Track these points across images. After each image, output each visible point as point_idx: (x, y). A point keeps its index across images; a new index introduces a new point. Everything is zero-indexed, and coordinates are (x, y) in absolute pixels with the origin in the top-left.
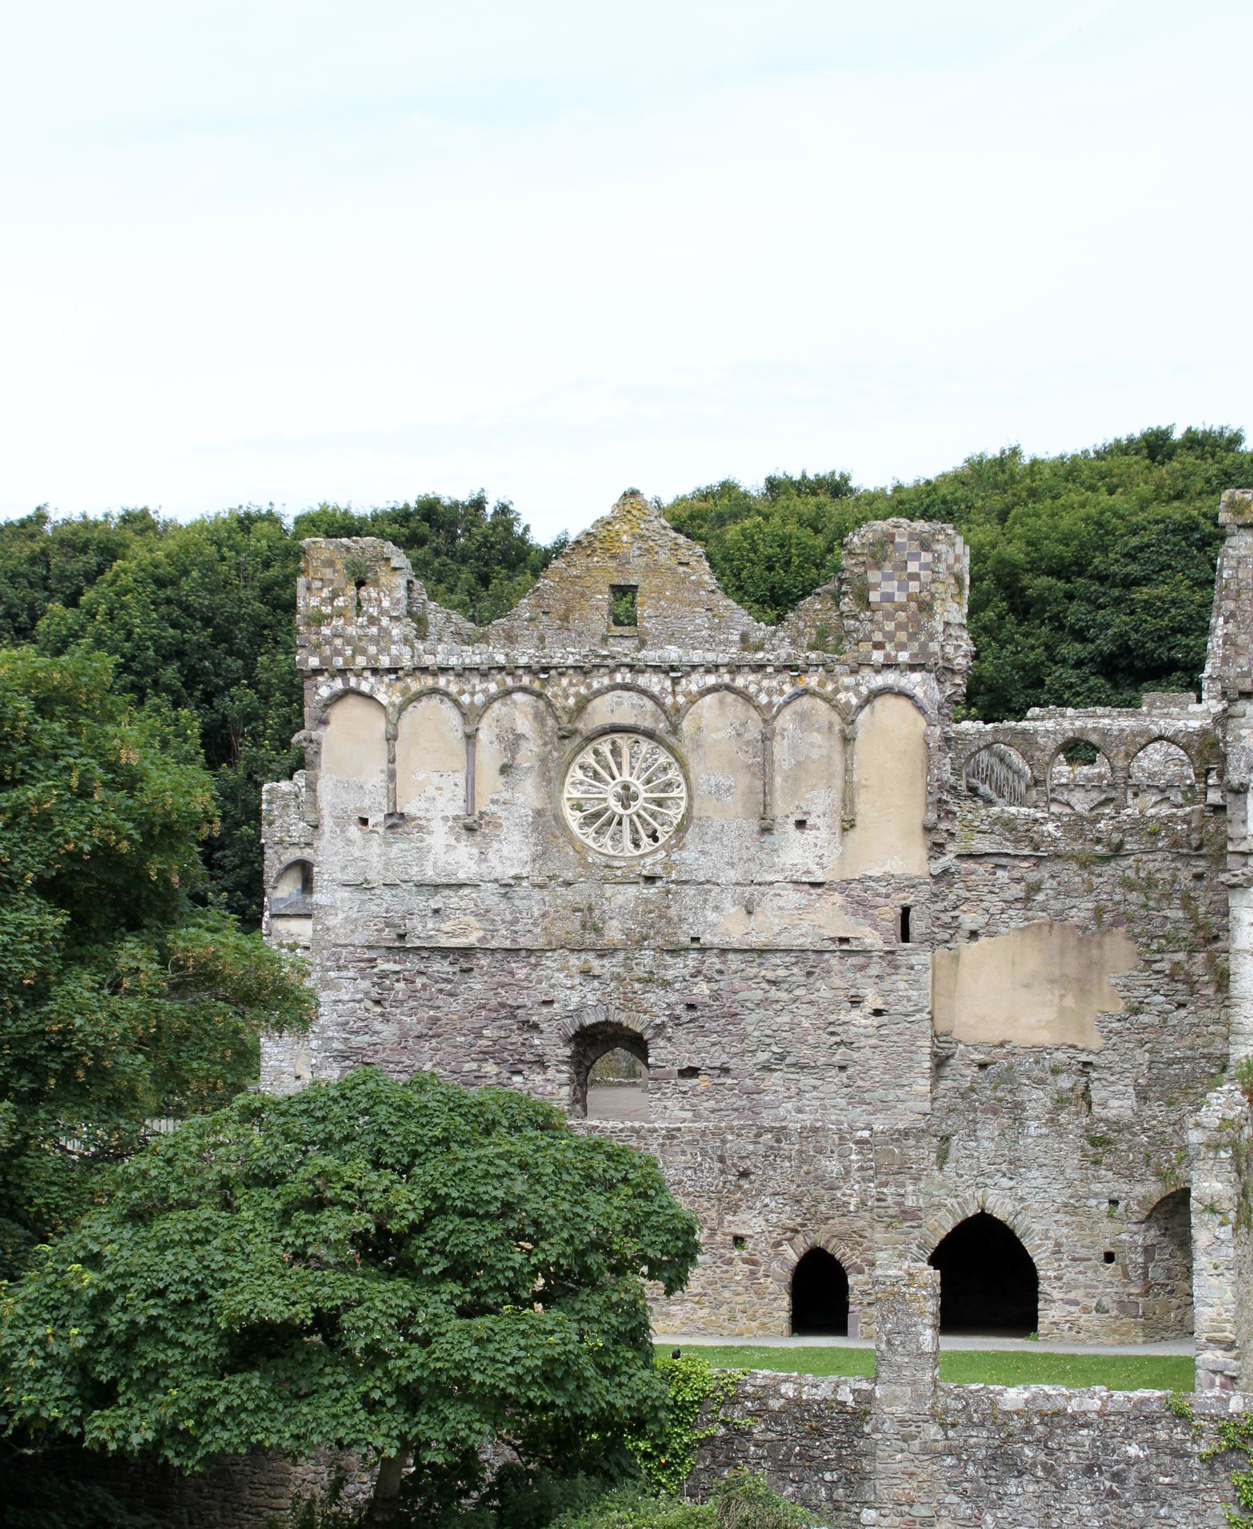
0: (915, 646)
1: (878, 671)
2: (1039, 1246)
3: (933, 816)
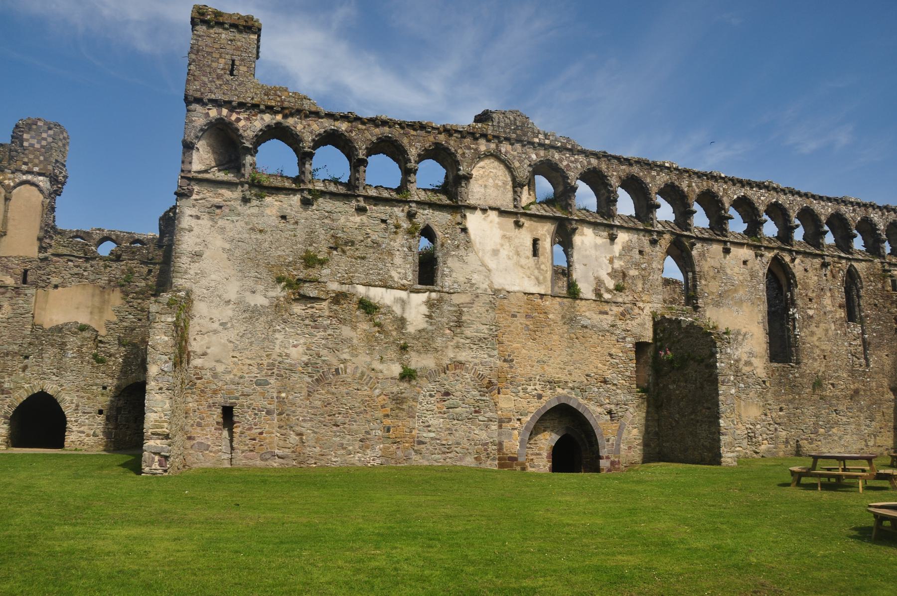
0: (42, 166)
1: (24, 174)
2: (68, 407)
3: (42, 234)
